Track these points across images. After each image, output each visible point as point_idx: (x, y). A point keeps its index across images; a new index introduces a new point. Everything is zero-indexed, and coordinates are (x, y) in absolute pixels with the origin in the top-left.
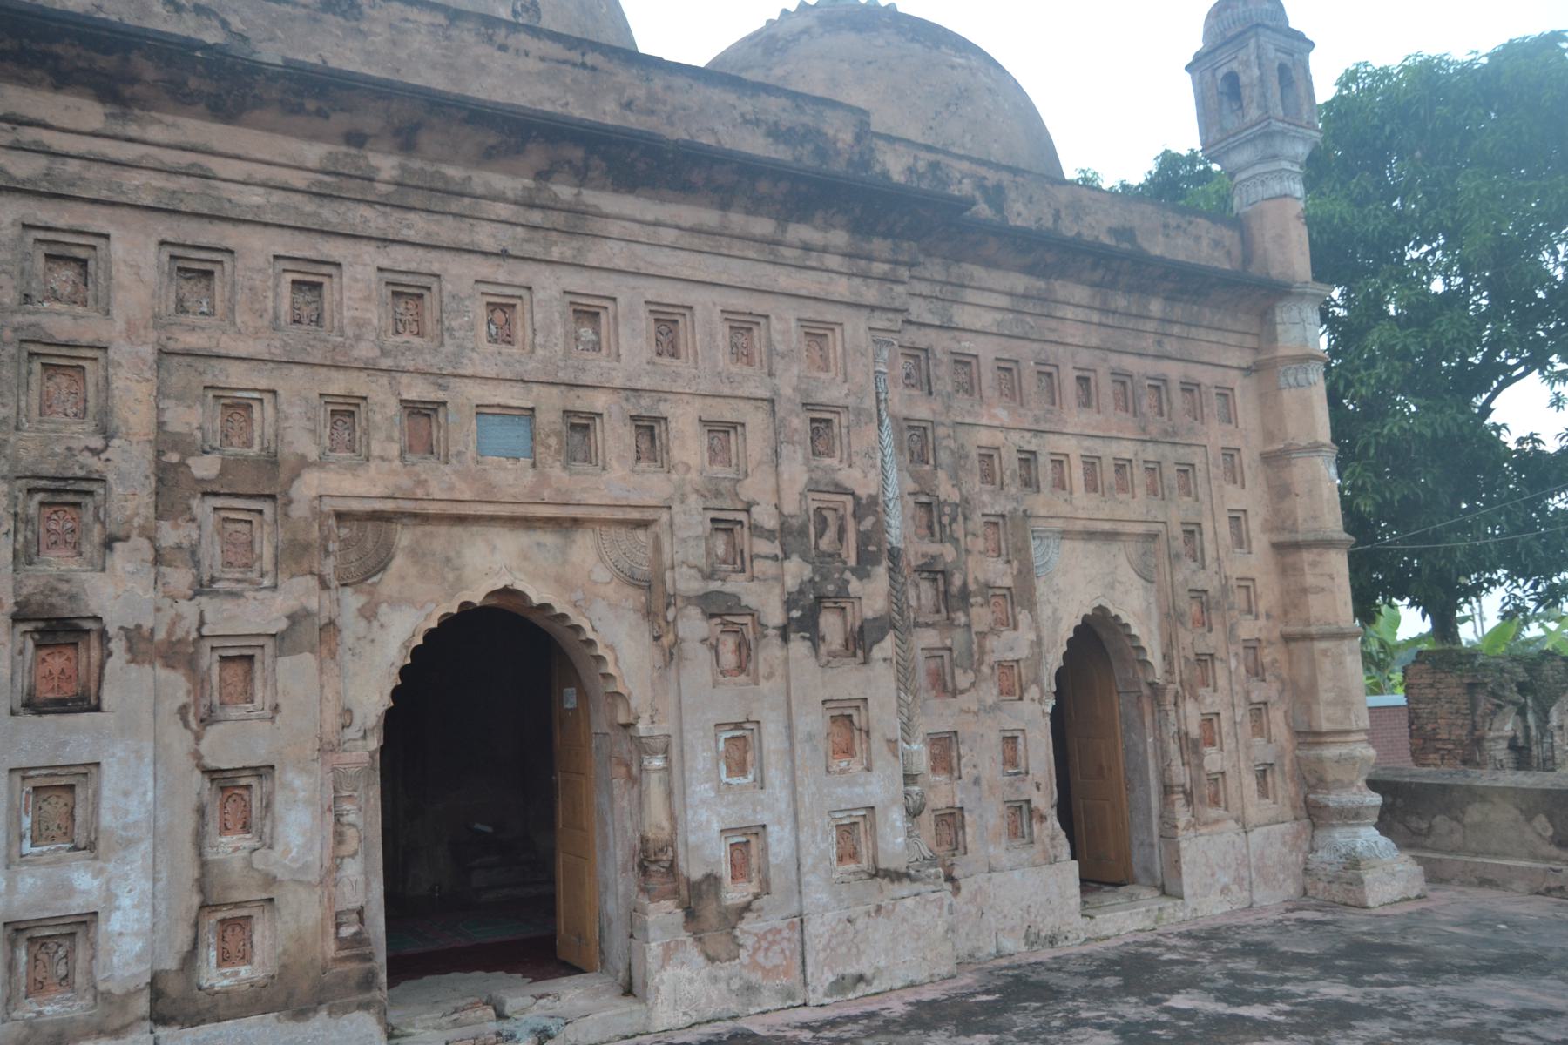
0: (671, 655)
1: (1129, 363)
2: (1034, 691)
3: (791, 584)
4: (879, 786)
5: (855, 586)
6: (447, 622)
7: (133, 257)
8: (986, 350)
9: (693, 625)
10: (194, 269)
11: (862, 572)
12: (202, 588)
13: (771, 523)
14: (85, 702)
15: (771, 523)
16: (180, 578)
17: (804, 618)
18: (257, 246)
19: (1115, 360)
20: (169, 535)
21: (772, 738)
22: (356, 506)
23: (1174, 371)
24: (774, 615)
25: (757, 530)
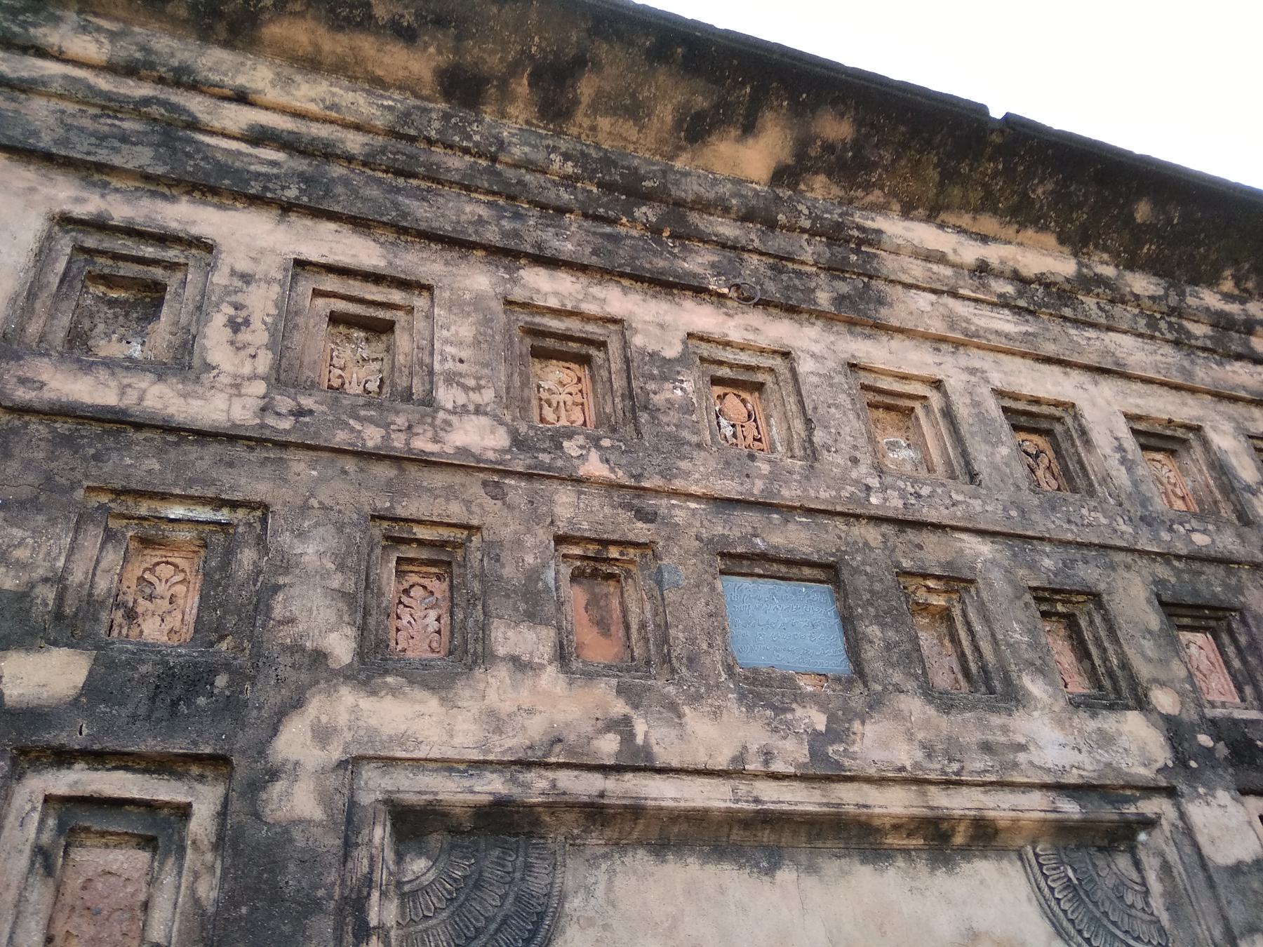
22: (450, 790)
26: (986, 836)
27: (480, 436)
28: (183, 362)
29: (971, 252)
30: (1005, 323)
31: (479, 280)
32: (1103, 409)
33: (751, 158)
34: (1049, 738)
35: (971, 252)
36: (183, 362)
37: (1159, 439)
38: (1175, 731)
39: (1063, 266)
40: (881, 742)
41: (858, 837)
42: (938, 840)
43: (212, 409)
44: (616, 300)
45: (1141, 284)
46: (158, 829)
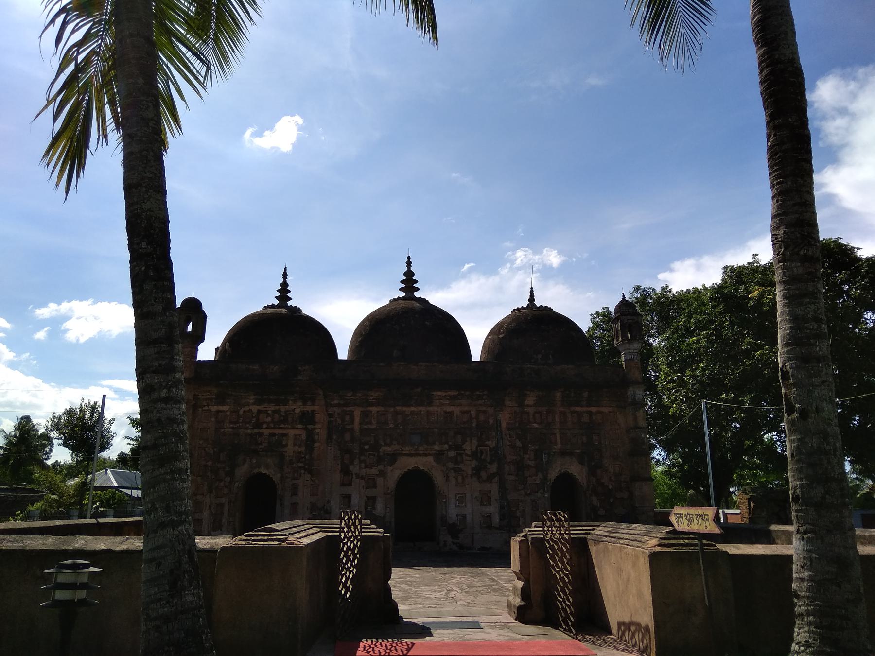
0: (447, 478)
1: (578, 409)
2: (542, 491)
3: (473, 466)
4: (493, 509)
5: (489, 466)
6: (406, 473)
7: (357, 413)
8: (531, 410)
9: (452, 474)
10: (365, 415)
11: (491, 463)
12: (366, 467)
13: (469, 453)
14: (350, 485)
15: (469, 453)
16: (363, 465)
17: (477, 472)
18: (374, 409)
19: (573, 408)
20: (362, 458)
21: (468, 495)
23: (594, 409)
24: (469, 472)
25: (467, 455)
26: (429, 455)
27: (392, 426)
28: (371, 423)
29: (444, 394)
30: (448, 402)
31: (392, 410)
32: (456, 410)
33: (419, 390)
34: (437, 447)
35: (444, 394)
36: (371, 423)
37: (463, 412)
38: (450, 446)
39: (456, 393)
40: (421, 448)
41: (420, 455)
42: (426, 455)
43: (375, 427)
44: (404, 409)
45: (467, 393)
46: (374, 455)
